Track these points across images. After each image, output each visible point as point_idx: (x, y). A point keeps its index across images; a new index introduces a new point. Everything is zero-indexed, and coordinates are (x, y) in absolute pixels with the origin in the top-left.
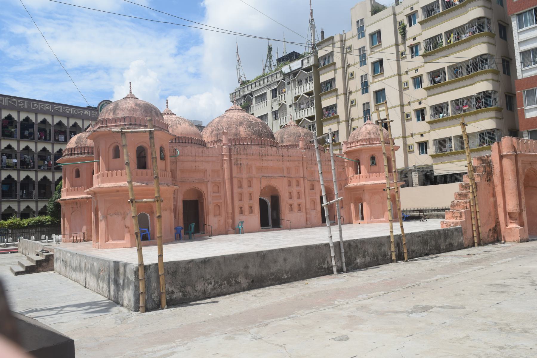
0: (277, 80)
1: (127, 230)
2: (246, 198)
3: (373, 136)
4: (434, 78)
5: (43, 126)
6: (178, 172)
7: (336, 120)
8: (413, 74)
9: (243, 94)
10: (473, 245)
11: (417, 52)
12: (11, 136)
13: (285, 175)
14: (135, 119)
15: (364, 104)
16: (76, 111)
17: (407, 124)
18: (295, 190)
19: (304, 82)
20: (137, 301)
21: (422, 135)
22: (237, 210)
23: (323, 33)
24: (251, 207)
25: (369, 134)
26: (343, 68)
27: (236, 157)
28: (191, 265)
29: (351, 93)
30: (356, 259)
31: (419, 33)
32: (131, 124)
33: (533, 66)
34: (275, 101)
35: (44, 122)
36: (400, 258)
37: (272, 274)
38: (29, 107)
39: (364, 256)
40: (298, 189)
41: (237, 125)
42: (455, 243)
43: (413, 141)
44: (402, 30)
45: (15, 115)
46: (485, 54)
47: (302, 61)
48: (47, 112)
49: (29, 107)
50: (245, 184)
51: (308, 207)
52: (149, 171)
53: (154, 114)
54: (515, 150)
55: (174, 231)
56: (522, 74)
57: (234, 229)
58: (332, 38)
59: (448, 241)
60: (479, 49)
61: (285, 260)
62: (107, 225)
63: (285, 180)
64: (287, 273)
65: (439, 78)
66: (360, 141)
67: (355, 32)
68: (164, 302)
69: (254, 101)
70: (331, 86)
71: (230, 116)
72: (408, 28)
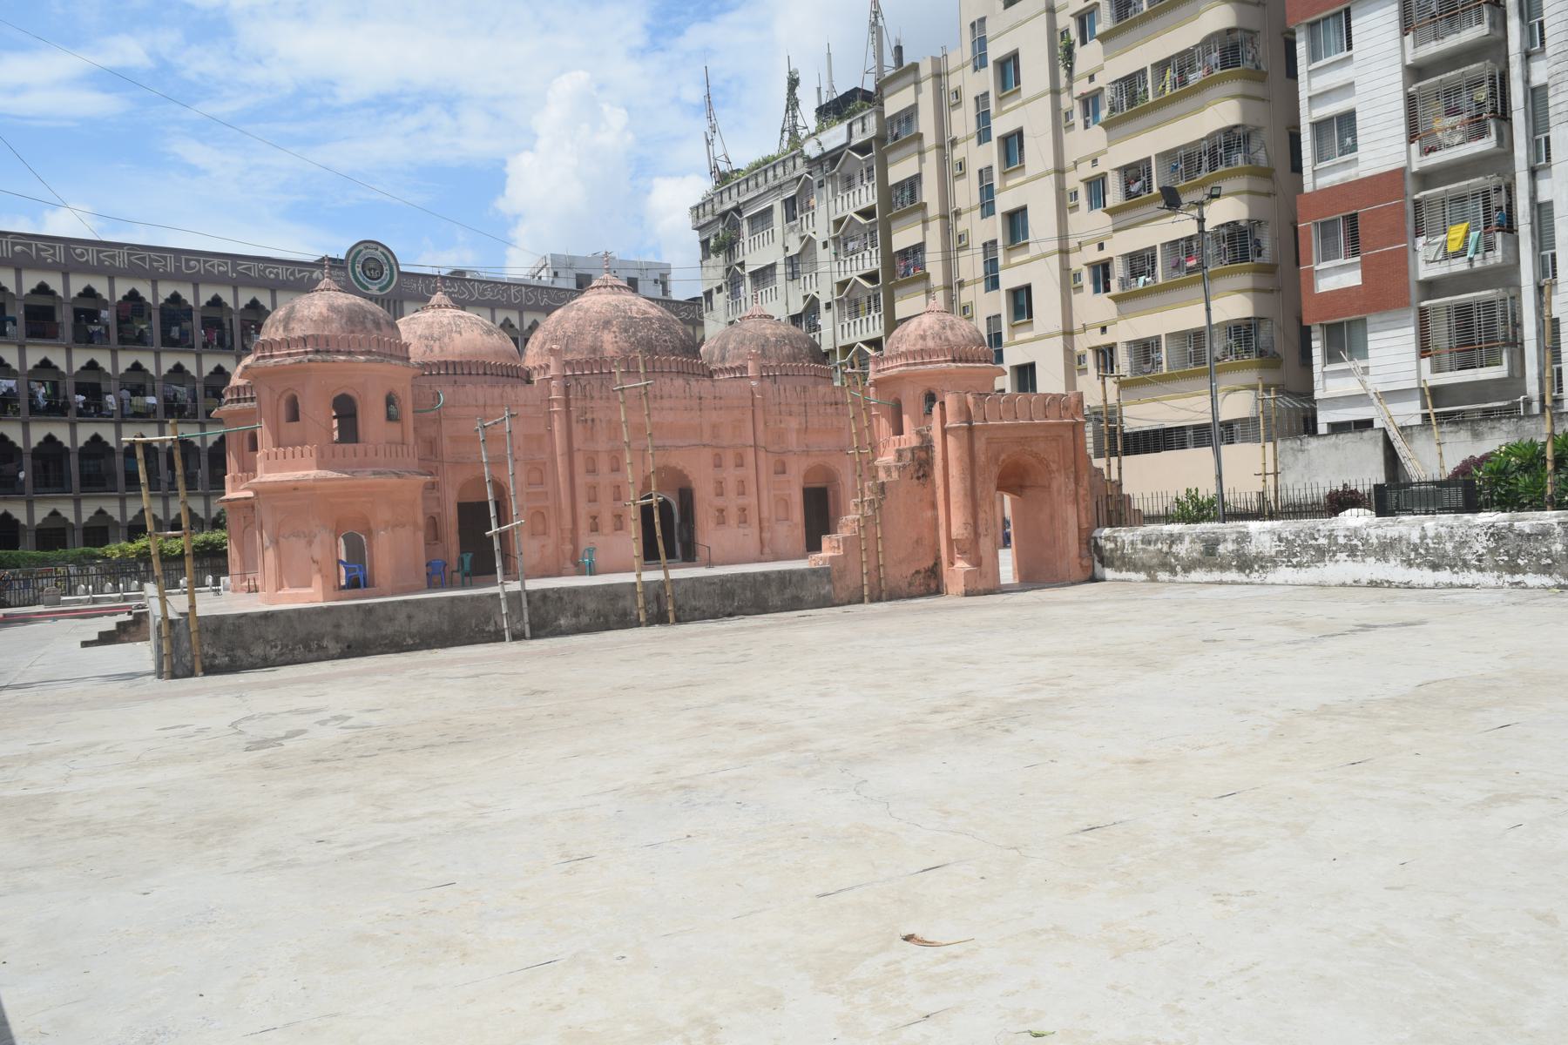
0: (797, 174)
1: (315, 567)
2: (605, 496)
3: (931, 344)
4: (1128, 184)
5: (214, 313)
6: (446, 442)
7: (922, 285)
8: (1087, 171)
9: (719, 209)
10: (861, 601)
11: (1096, 114)
12: (140, 341)
13: (707, 439)
14: (327, 340)
15: (985, 245)
16: (292, 274)
17: (1076, 298)
18: (731, 475)
19: (858, 180)
20: (160, 665)
21: (1104, 329)
22: (584, 524)
23: (899, 49)
24: (619, 517)
25: (923, 338)
26: (940, 147)
27: (580, 404)
28: (243, 621)
29: (958, 214)
30: (556, 619)
31: (1102, 65)
32: (317, 352)
33: (1338, 160)
34: (792, 229)
35: (216, 302)
36: (660, 618)
37: (385, 637)
38: (178, 268)
39: (576, 615)
40: (739, 472)
41: (597, 328)
42: (808, 595)
43: (1085, 343)
44: (1063, 55)
45: (145, 291)
46: (1236, 127)
47: (850, 126)
48: (221, 280)
49: (178, 268)
50: (604, 465)
51: (765, 514)
52: (358, 447)
53: (369, 325)
54: (969, 420)
55: (424, 570)
56: (1314, 178)
57: (577, 564)
58: (915, 67)
59: (788, 593)
60: (1220, 113)
61: (410, 617)
62: (279, 556)
63: (707, 456)
64: (412, 636)
65: (1138, 184)
66: (900, 355)
67: (968, 54)
68: (198, 667)
69: (745, 228)
70: (913, 197)
71: (586, 306)
72: (1077, 49)
